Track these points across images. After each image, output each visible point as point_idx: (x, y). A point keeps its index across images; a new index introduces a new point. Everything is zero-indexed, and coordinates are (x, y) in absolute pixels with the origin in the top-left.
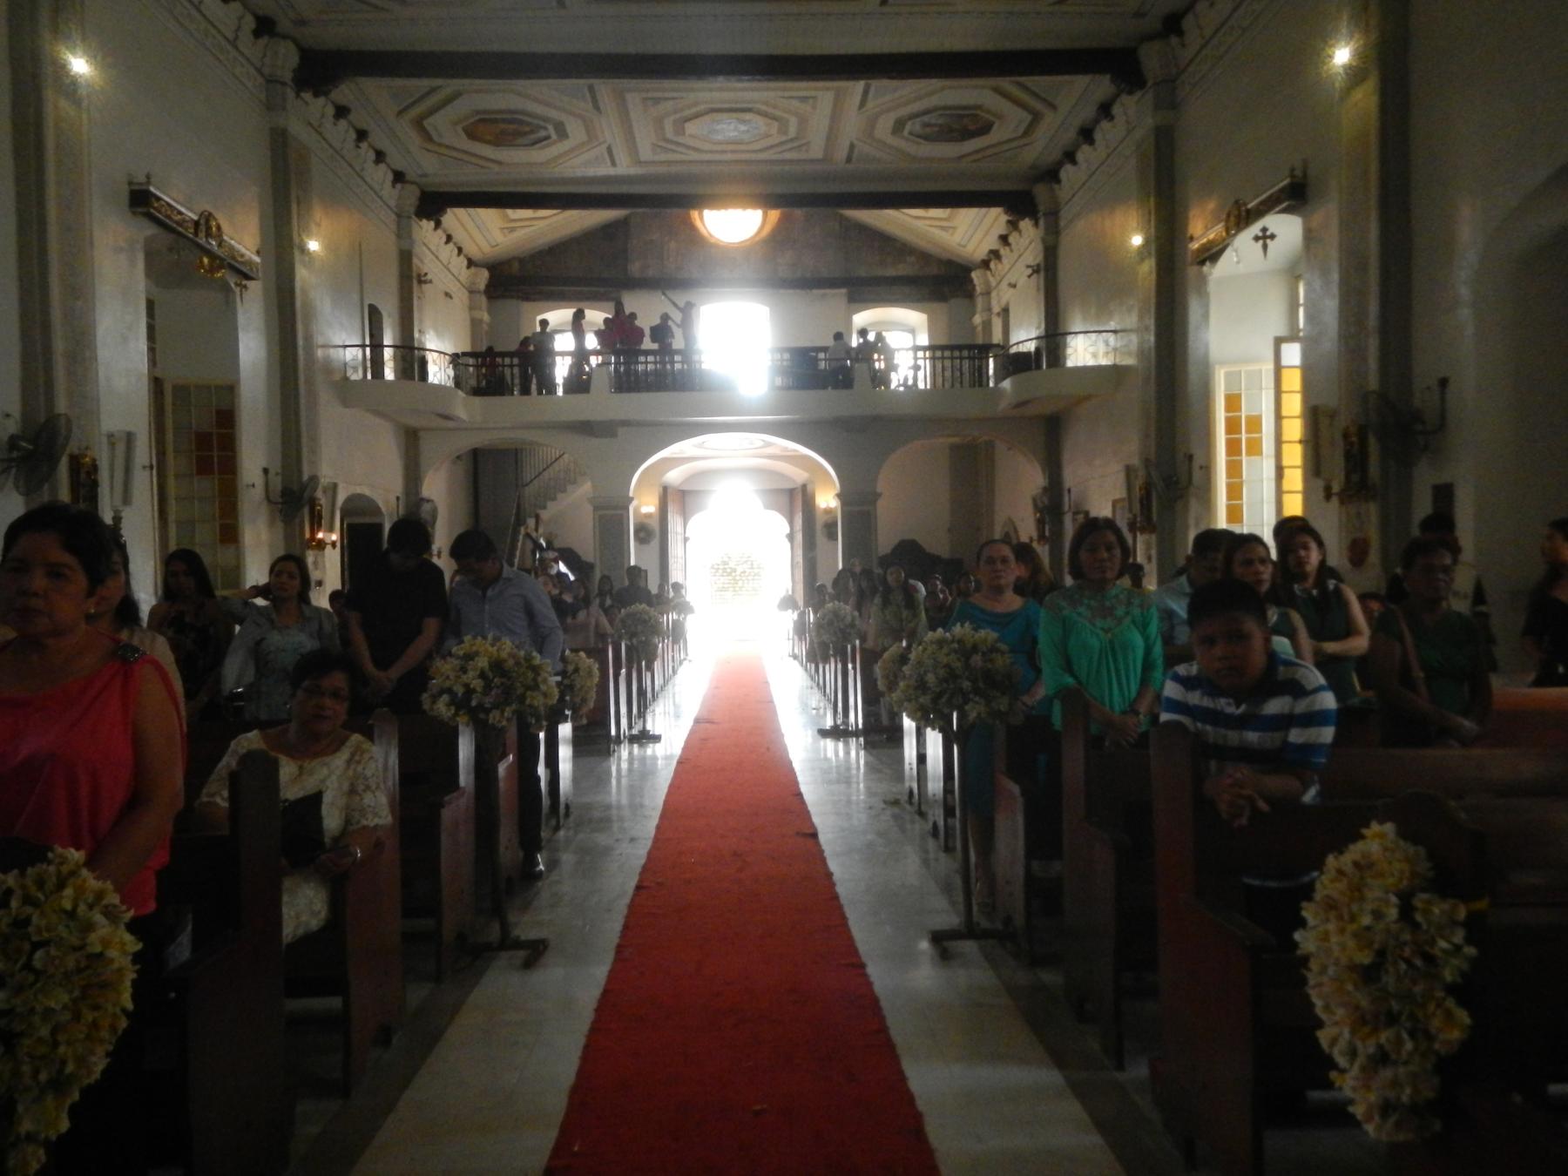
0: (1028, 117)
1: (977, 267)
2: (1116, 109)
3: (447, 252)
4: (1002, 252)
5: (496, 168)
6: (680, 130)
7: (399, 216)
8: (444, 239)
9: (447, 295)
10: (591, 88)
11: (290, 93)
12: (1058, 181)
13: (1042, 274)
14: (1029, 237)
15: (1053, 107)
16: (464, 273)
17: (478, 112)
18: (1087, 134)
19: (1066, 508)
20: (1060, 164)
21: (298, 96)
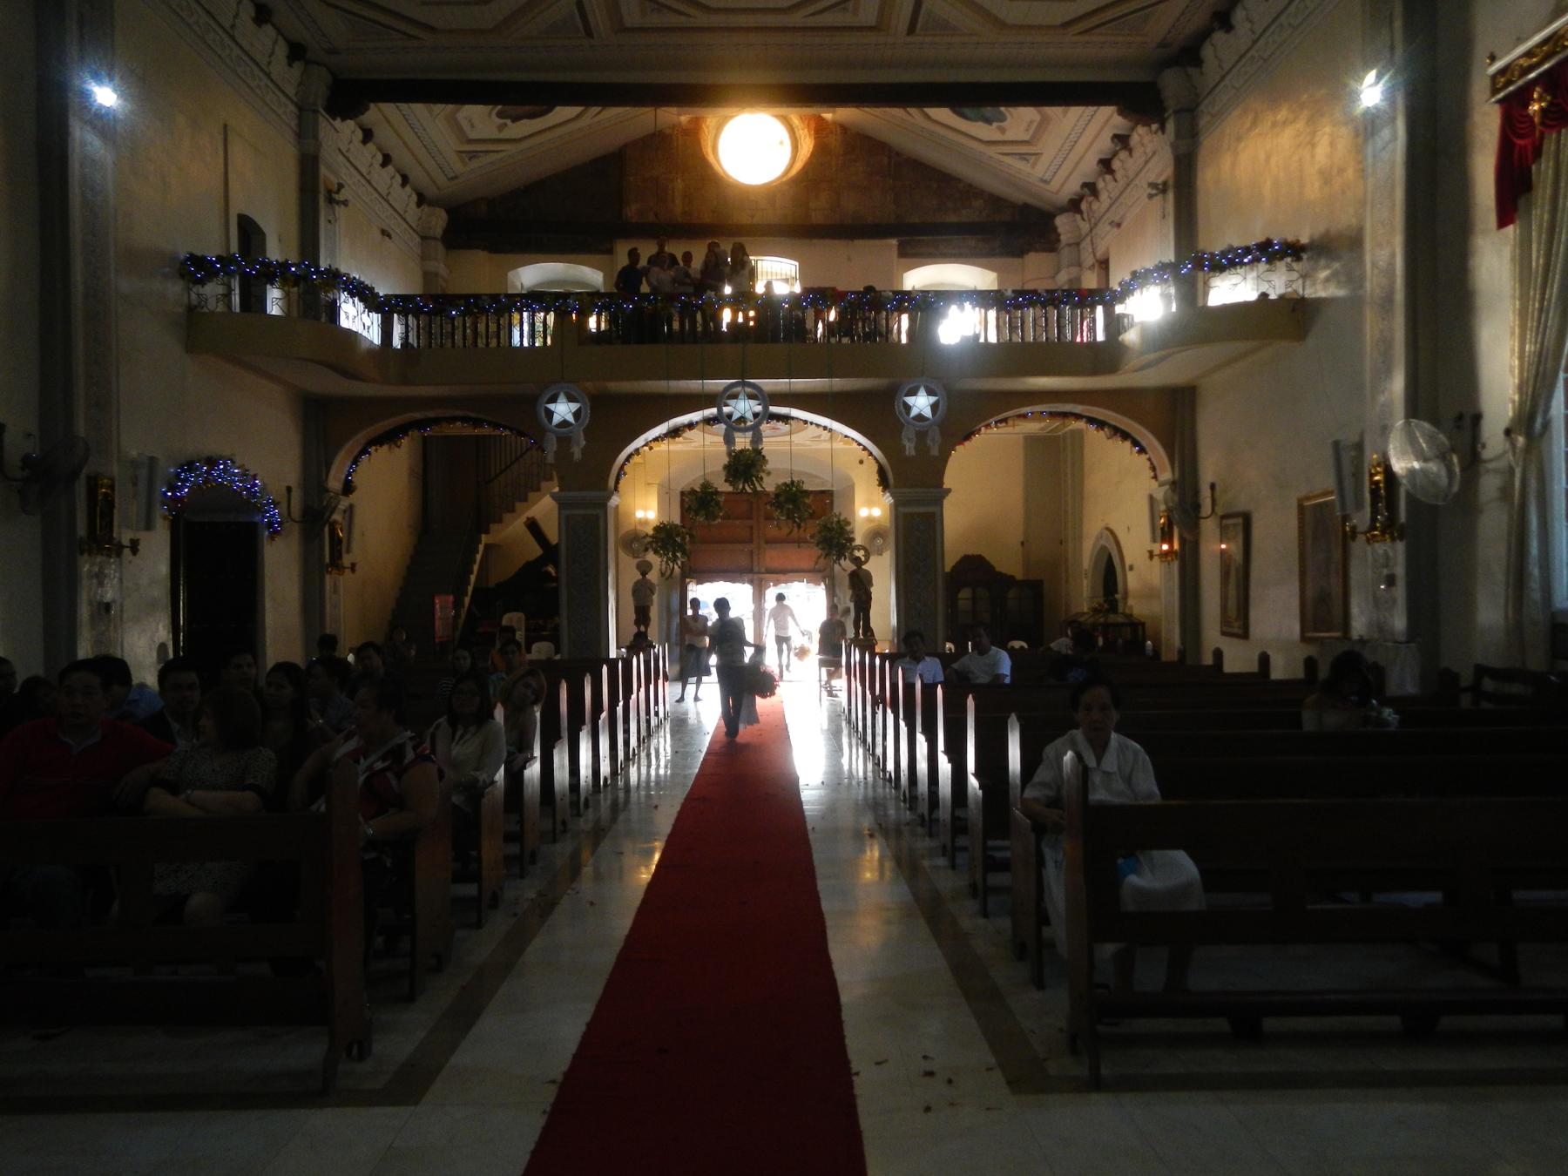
1: (1062, 210)
3: (385, 178)
4: (1100, 185)
7: (300, 109)
9: (384, 233)
12: (1197, 62)
13: (1171, 195)
14: (1153, 151)
16: (413, 212)
19: (1206, 508)
20: (1204, 35)
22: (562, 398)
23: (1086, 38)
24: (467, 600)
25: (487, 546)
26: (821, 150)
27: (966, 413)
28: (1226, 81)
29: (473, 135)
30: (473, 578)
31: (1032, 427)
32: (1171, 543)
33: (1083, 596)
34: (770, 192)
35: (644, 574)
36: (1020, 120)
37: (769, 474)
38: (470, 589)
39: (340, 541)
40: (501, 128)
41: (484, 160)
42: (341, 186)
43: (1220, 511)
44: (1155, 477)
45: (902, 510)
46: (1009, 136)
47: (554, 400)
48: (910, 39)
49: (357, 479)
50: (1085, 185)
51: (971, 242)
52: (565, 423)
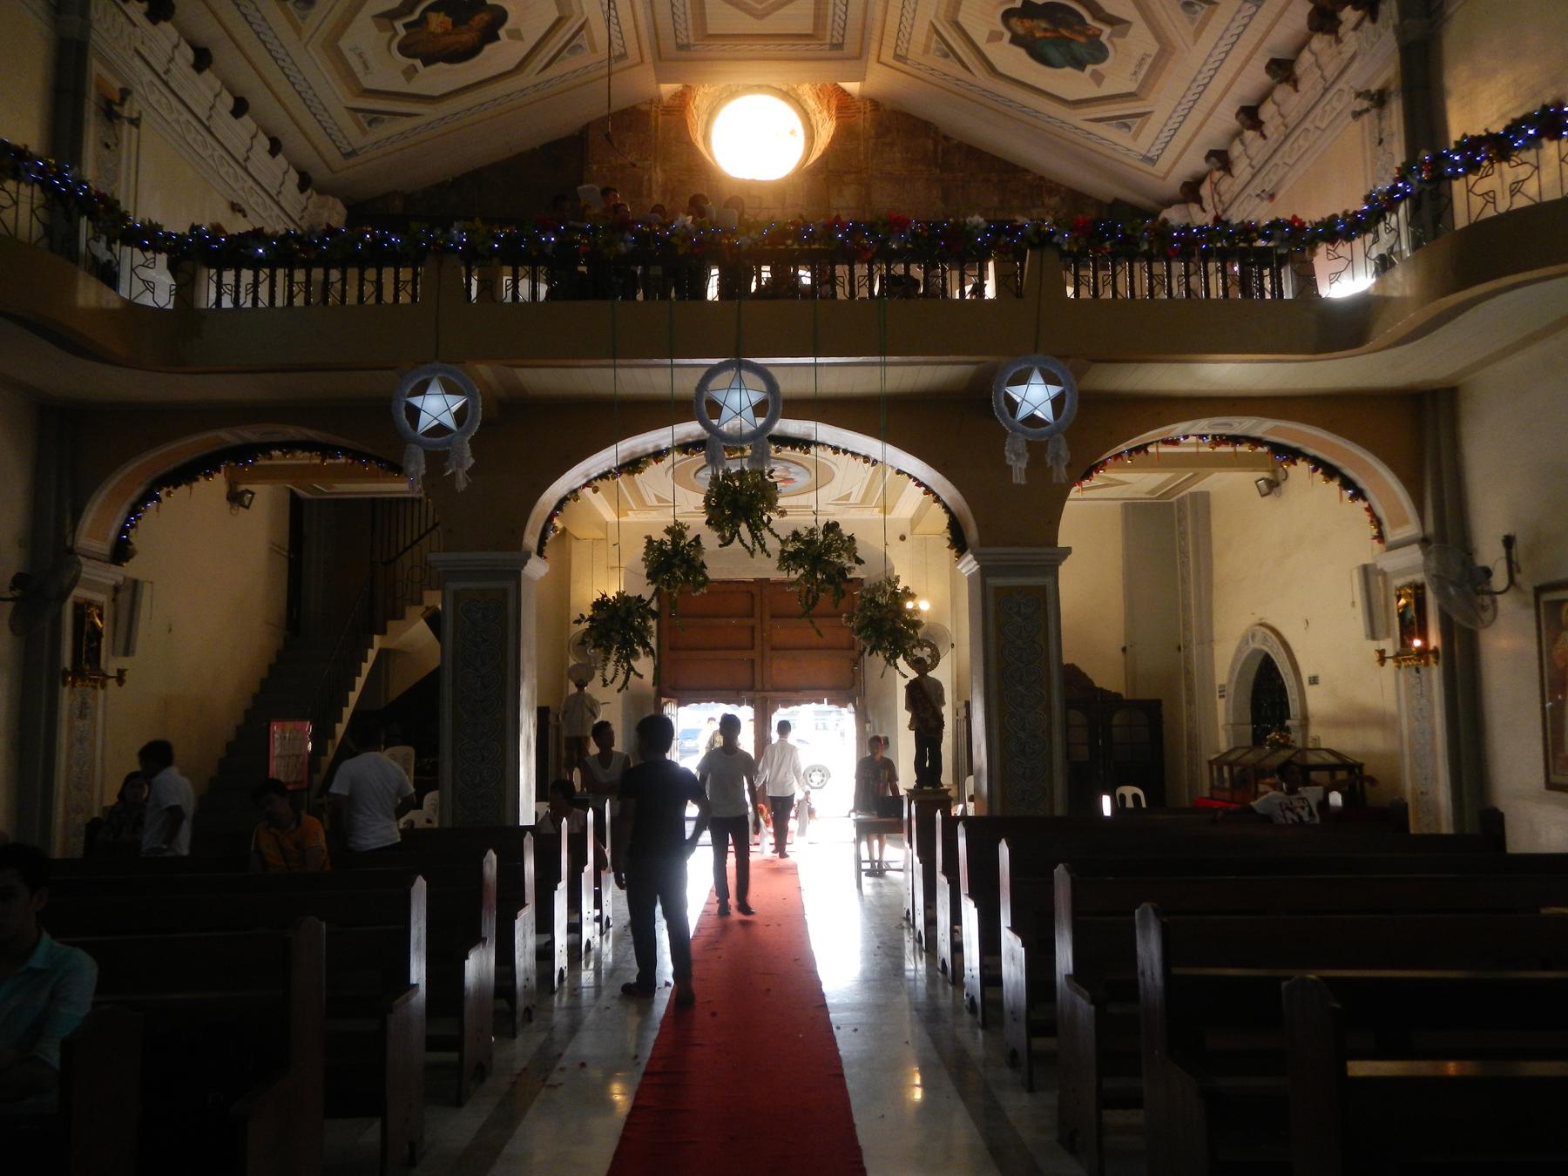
4: (1236, 150)
13: (1395, 108)
19: (1499, 580)
22: (435, 386)
24: (340, 729)
25: (383, 654)
26: (844, 134)
27: (1100, 427)
29: (369, 82)
30: (353, 697)
32: (1424, 636)
33: (1220, 724)
35: (581, 685)
37: (783, 513)
38: (347, 713)
39: (97, 634)
40: (410, 73)
42: (125, 93)
43: (1526, 581)
44: (1380, 537)
45: (995, 582)
46: (1107, 89)
47: (421, 390)
49: (137, 538)
50: (1212, 154)
52: (440, 430)
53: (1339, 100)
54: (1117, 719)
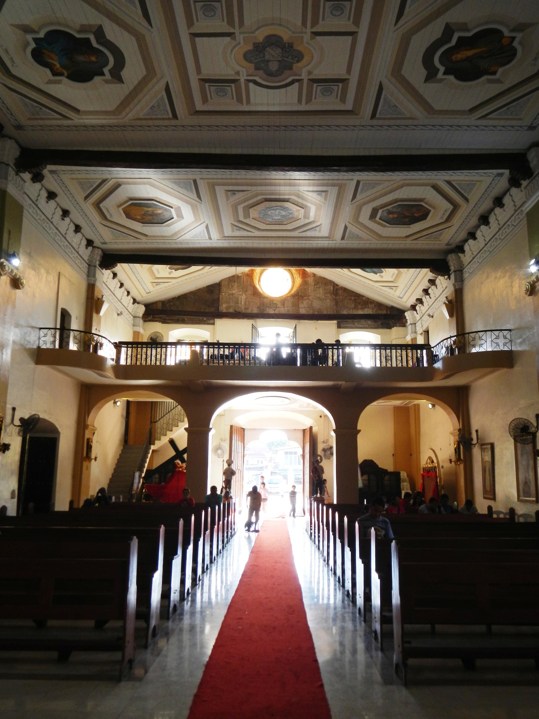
0: (450, 207)
2: (507, 200)
3: (121, 293)
4: (424, 299)
5: (144, 239)
6: (247, 215)
7: (89, 265)
8: (119, 285)
10: (195, 181)
11: (11, 172)
12: (463, 252)
14: (444, 286)
15: (467, 200)
16: (131, 307)
17: (131, 199)
18: (484, 220)
19: (475, 441)
20: (466, 241)
21: (17, 174)
23: (415, 242)
25: (153, 451)
28: (475, 259)
31: (398, 403)
34: (283, 301)
36: (389, 273)
38: (145, 470)
40: (170, 273)
41: (162, 286)
48: (343, 242)
51: (369, 322)
53: (508, 229)
54: (386, 478)
